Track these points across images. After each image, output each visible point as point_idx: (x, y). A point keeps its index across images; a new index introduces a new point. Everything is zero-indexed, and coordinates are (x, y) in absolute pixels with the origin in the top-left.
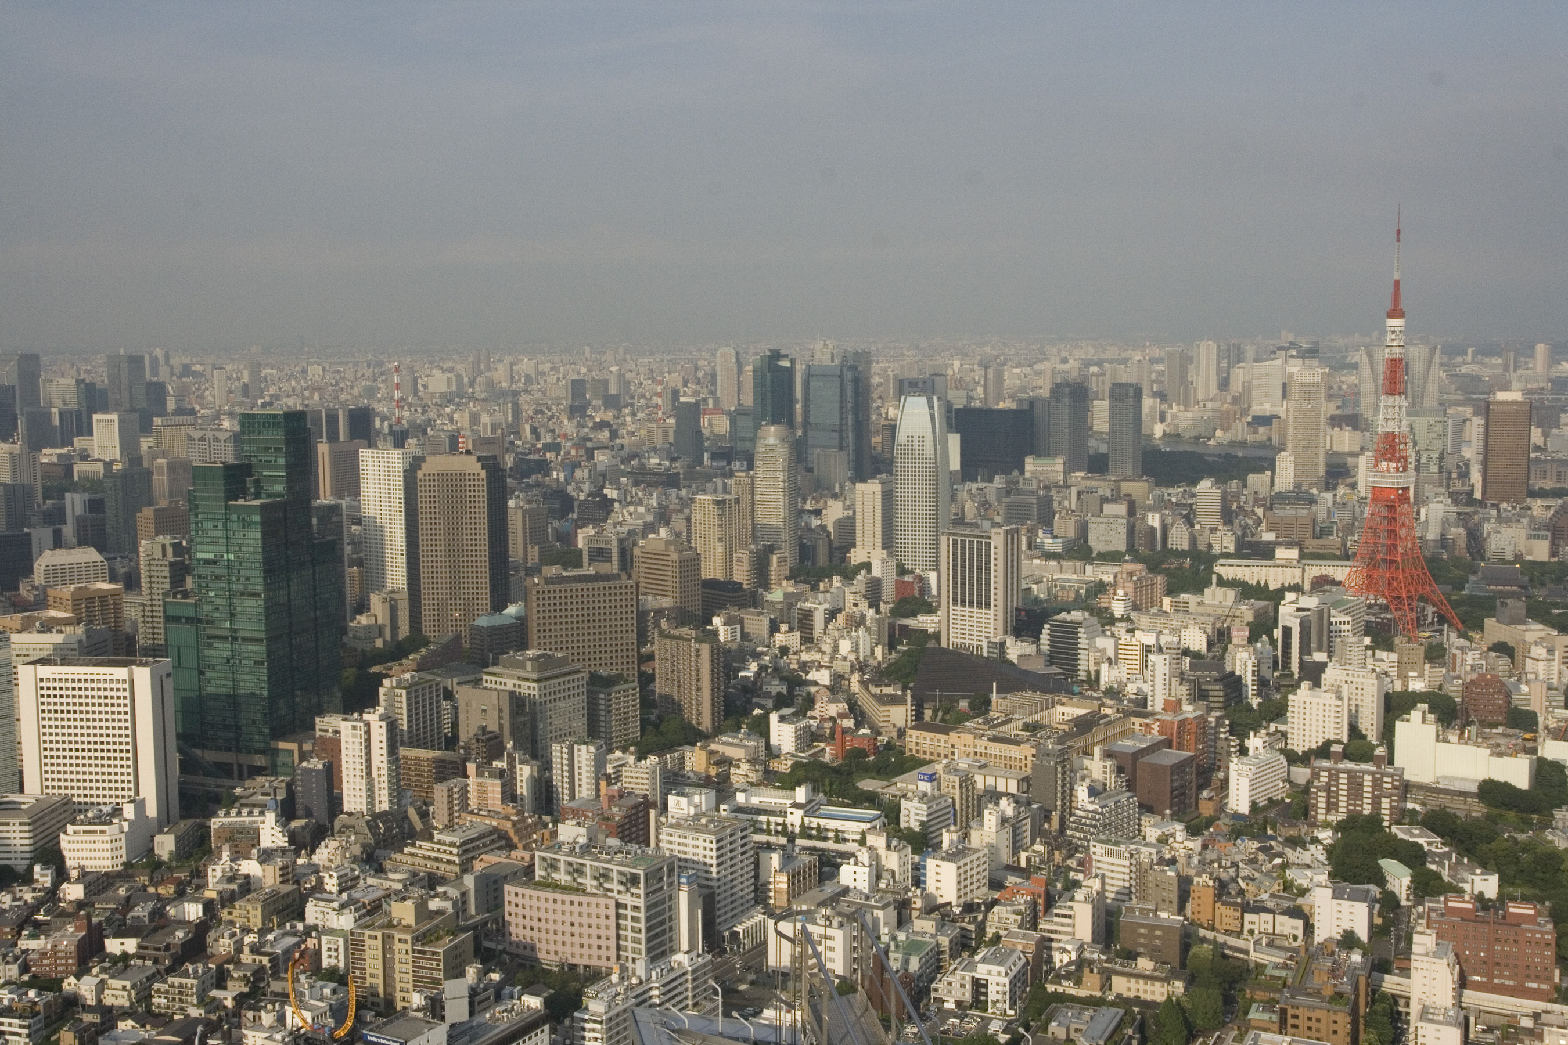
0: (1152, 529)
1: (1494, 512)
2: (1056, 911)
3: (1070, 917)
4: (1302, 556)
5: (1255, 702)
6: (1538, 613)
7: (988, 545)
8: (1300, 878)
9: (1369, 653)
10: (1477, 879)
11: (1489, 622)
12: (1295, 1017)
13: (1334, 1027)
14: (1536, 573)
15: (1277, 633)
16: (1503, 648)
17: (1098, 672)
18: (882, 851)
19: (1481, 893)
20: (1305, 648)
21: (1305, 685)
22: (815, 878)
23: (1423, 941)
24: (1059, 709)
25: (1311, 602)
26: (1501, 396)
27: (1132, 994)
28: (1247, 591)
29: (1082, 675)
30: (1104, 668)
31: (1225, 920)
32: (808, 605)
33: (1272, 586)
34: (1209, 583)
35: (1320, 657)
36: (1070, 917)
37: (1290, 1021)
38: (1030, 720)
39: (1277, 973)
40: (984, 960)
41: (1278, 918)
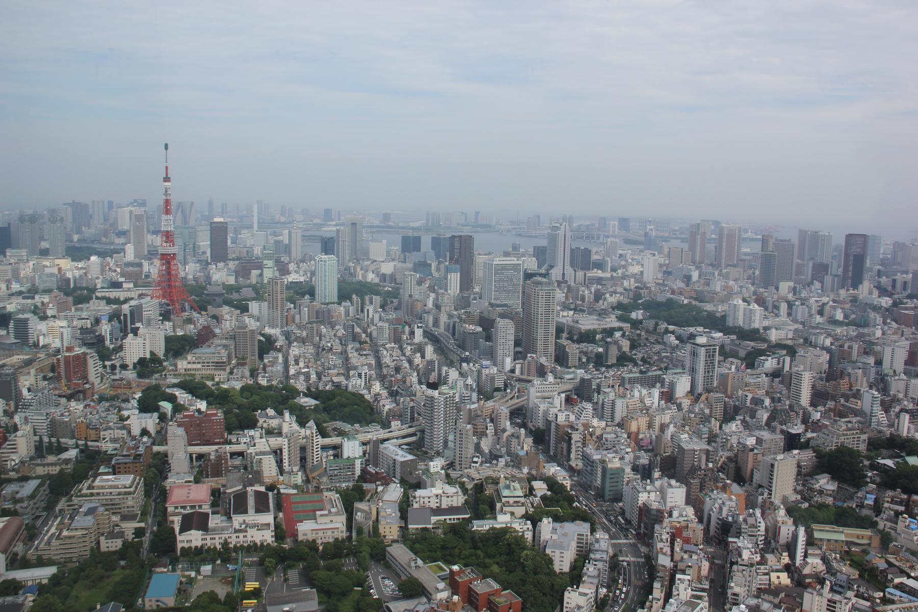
1: (214, 266)
2: (7, 443)
3: (15, 444)
4: (135, 286)
9: (160, 322)
10: (198, 404)
11: (209, 307)
12: (119, 468)
13: (136, 469)
14: (230, 289)
15: (122, 317)
16: (215, 317)
17: (38, 340)
19: (200, 409)
21: (131, 335)
24: (16, 357)
25: (133, 303)
26: (216, 220)
27: (46, 473)
28: (109, 301)
29: (31, 342)
30: (41, 338)
31: (92, 436)
33: (122, 299)
34: (91, 298)
35: (138, 325)
36: (15, 444)
37: (117, 470)
39: (113, 452)
41: (116, 431)
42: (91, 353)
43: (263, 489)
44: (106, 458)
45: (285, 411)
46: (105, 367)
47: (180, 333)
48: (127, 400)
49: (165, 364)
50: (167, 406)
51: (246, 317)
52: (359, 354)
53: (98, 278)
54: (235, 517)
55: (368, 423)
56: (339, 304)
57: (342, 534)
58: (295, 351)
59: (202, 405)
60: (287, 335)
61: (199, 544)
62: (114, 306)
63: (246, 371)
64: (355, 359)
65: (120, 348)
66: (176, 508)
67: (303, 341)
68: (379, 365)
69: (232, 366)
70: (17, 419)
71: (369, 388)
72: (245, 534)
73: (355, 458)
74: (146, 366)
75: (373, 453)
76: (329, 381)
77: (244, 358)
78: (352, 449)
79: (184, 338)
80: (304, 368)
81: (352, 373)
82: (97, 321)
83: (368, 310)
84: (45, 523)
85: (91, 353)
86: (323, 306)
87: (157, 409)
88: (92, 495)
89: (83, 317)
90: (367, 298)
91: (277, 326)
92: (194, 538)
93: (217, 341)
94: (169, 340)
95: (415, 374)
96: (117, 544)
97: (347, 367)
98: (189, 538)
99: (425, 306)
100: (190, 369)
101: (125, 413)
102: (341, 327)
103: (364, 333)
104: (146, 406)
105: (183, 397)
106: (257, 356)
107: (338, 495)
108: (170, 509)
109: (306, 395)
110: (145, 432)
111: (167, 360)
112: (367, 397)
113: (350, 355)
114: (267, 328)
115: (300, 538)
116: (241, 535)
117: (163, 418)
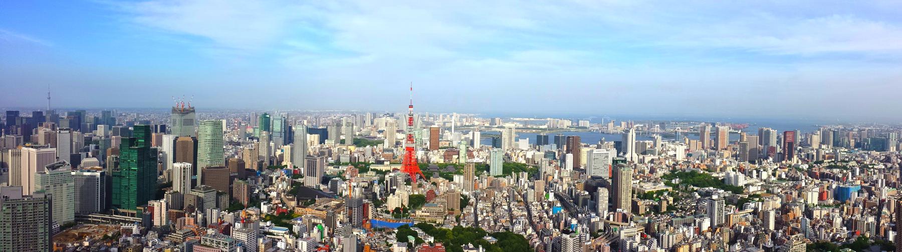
0: (356, 157)
4: (390, 163)
5: (380, 199)
6: (441, 175)
7: (316, 161)
8: (390, 242)
14: (441, 166)
15: (385, 182)
16: (434, 184)
17: (342, 192)
18: (288, 239)
19: (430, 242)
20: (391, 186)
21: (391, 194)
22: (271, 246)
24: (333, 202)
25: (392, 174)
26: (433, 126)
30: (344, 191)
32: (272, 176)
33: (384, 170)
34: (368, 170)
35: (394, 187)
38: (325, 205)
42: (371, 203)
45: (480, 246)
47: (416, 193)
48: (390, 233)
49: (409, 211)
50: (412, 239)
51: (452, 185)
52: (518, 208)
53: (370, 158)
56: (504, 177)
58: (480, 205)
59: (432, 239)
60: (476, 195)
62: (381, 175)
65: (386, 200)
67: (485, 200)
69: (446, 214)
70: (335, 240)
71: (525, 230)
74: (399, 212)
76: (501, 226)
77: (452, 210)
80: (486, 216)
81: (514, 221)
82: (372, 183)
83: (521, 181)
85: (371, 203)
86: (495, 178)
87: (407, 240)
89: (365, 180)
90: (520, 173)
93: (438, 200)
94: (411, 198)
95: (552, 221)
99: (553, 178)
100: (423, 216)
102: (506, 192)
103: (519, 195)
105: (420, 232)
106: (459, 209)
109: (490, 235)
111: (409, 209)
112: (525, 236)
113: (513, 209)
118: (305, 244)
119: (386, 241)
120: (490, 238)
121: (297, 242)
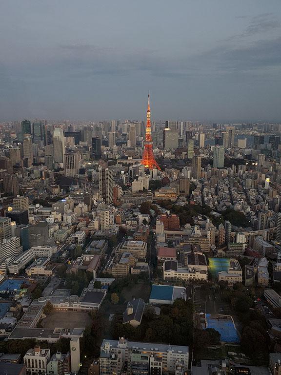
20: (134, 174)
21: (135, 180)
23: (158, 222)
25: (134, 166)
28: (124, 165)
35: (137, 175)
40: (77, 234)
41: (133, 221)
43: (201, 254)
44: (131, 233)
46: (124, 193)
48: (135, 208)
53: (116, 155)
54: (189, 266)
55: (245, 226)
56: (226, 169)
57: (240, 279)
58: (205, 190)
60: (201, 182)
61: (174, 276)
63: (185, 199)
64: (235, 194)
66: (162, 258)
68: (247, 199)
72: (194, 274)
73: (242, 244)
75: (250, 242)
78: (241, 239)
79: (157, 182)
81: (234, 201)
82: (119, 173)
84: (108, 259)
87: (149, 213)
88: (126, 248)
90: (240, 166)
91: (196, 178)
92: (170, 274)
96: (137, 271)
97: (232, 200)
98: (169, 273)
101: (136, 214)
104: (144, 211)
107: (237, 261)
108: (159, 258)
109: (214, 211)
110: (145, 222)
114: (192, 179)
115: (220, 279)
116: (193, 274)
117: (151, 217)
118: (69, 218)
119: (132, 213)
120: (215, 213)
121: (62, 218)
